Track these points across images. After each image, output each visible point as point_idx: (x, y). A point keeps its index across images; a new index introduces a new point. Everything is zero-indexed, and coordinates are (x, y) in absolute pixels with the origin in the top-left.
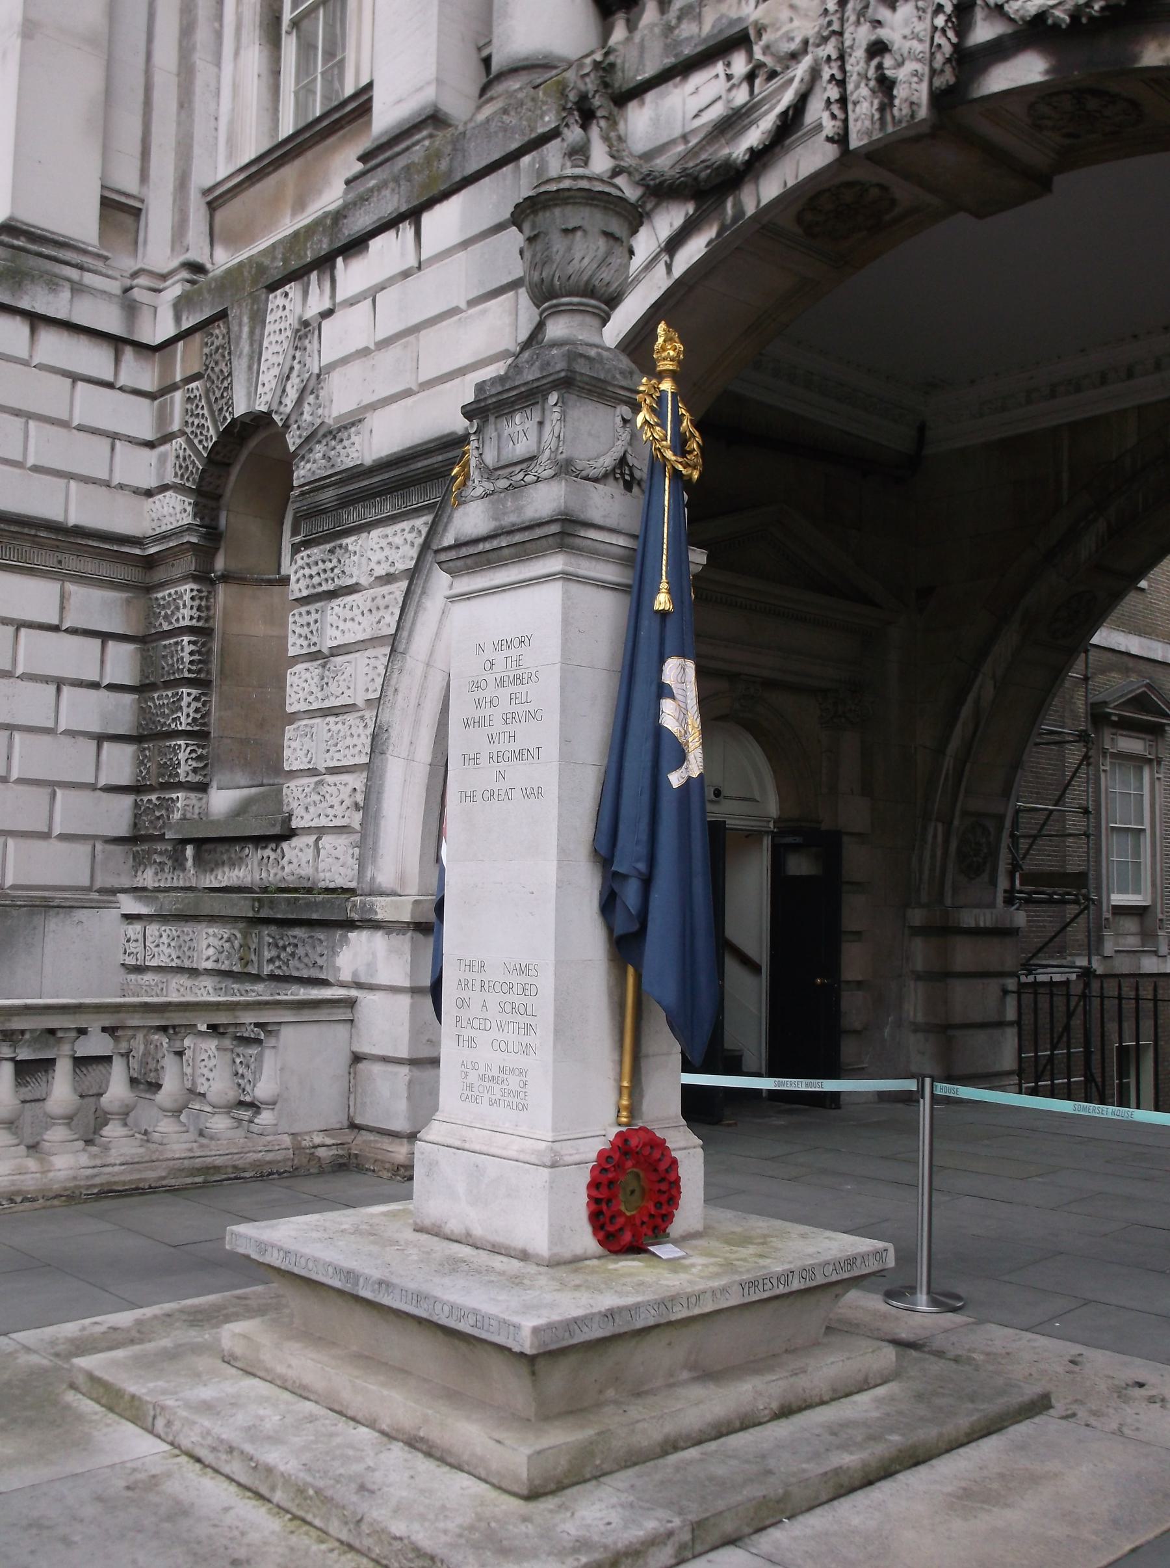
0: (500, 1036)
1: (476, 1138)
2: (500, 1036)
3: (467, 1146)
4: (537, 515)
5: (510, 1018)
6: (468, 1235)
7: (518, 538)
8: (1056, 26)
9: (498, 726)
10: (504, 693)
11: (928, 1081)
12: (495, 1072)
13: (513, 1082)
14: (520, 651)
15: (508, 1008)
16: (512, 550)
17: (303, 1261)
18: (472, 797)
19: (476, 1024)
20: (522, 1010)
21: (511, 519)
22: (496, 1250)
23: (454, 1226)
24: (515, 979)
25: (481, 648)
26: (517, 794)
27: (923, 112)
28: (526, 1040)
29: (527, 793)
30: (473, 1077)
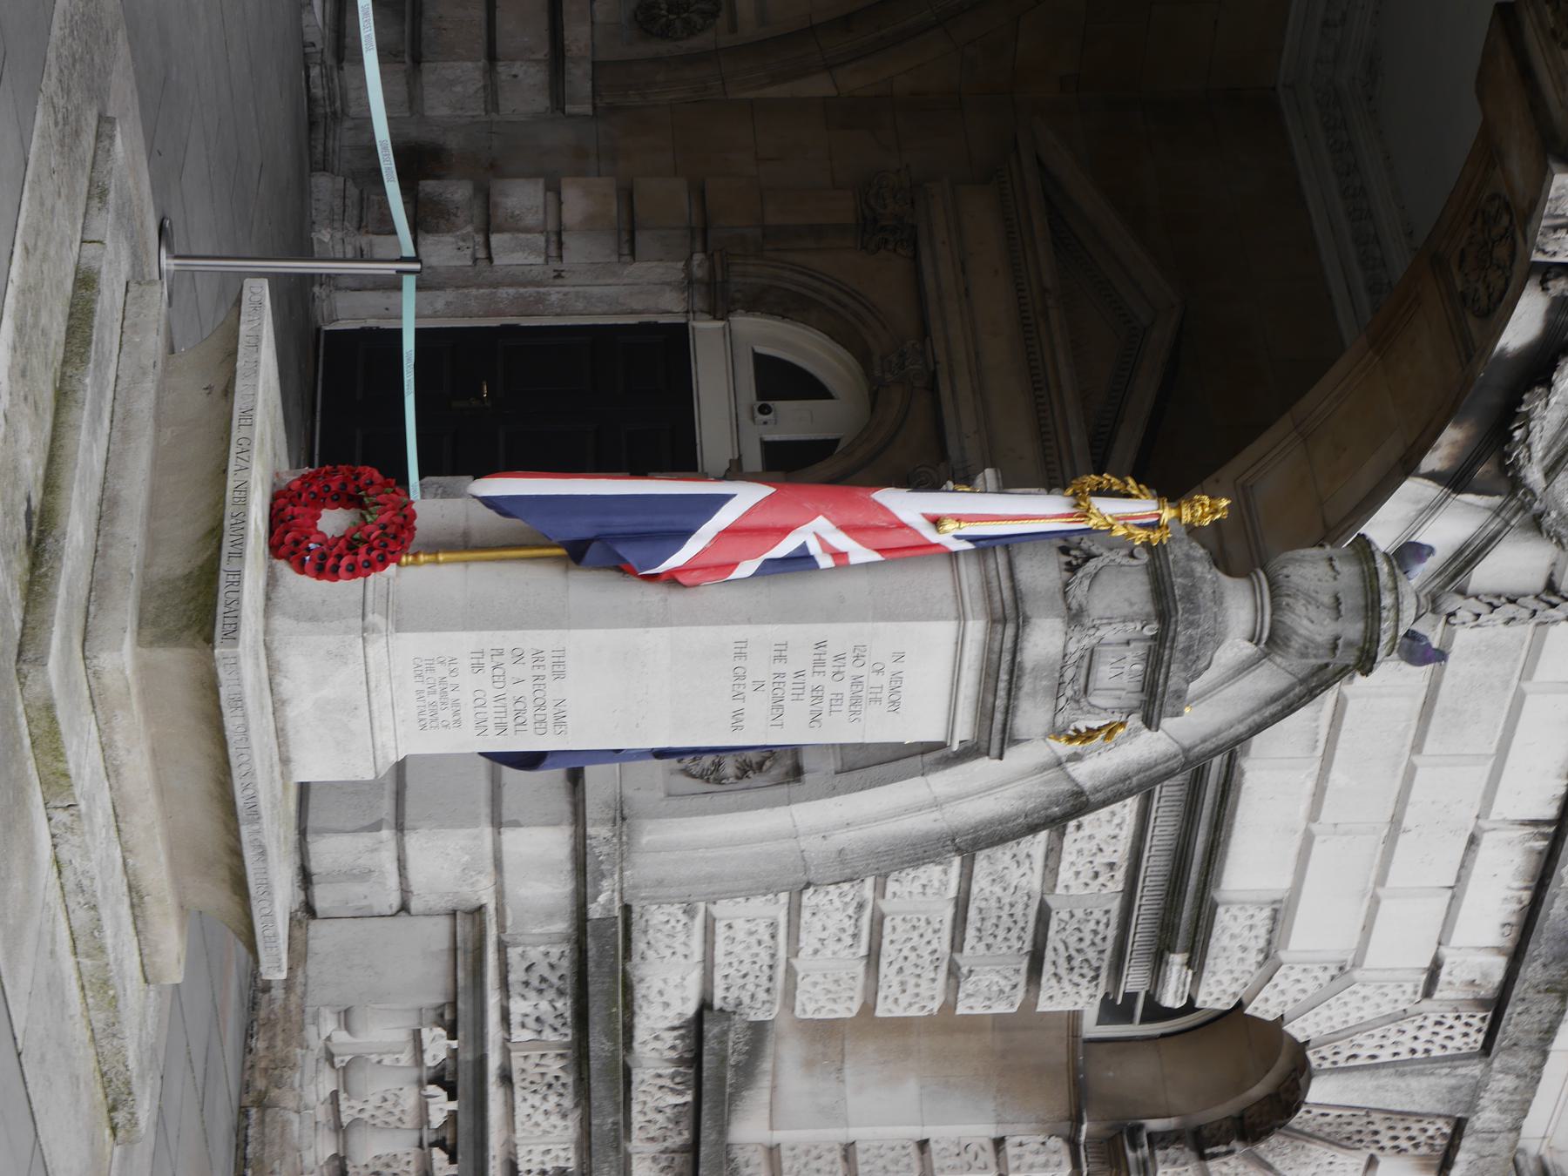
0: (490, 698)
1: (381, 698)
2: (490, 698)
3: (373, 695)
4: (1019, 713)
5: (511, 708)
6: (283, 703)
7: (999, 717)
8: (1529, 389)
9: (811, 681)
10: (845, 688)
11: (417, 266)
12: (452, 695)
13: (446, 715)
14: (885, 701)
15: (520, 706)
16: (989, 706)
17: (245, 758)
18: (740, 655)
19: (497, 672)
20: (520, 720)
21: (1027, 684)
22: (280, 733)
23: (286, 687)
24: (550, 711)
25: (900, 657)
26: (738, 705)
27: (1537, 257)
28: (490, 724)
29: (738, 714)
30: (442, 671)
